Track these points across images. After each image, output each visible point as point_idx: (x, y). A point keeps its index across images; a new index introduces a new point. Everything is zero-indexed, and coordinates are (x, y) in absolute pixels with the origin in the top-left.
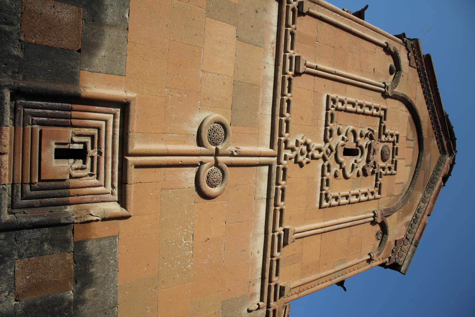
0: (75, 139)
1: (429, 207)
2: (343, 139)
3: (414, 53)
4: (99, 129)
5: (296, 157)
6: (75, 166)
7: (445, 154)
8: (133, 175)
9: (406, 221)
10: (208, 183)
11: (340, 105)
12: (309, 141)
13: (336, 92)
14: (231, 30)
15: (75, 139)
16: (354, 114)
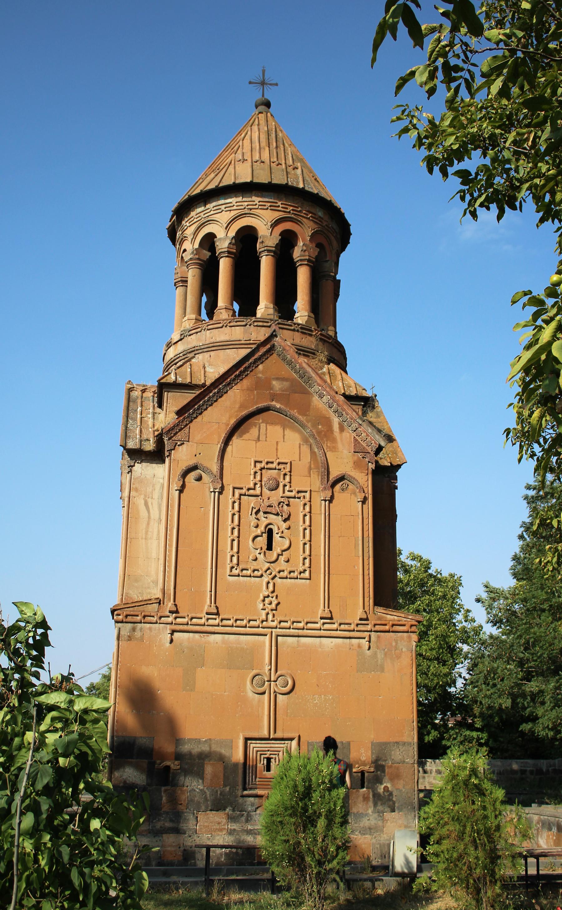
0: (262, 763)
1: (328, 389)
2: (260, 553)
3: (177, 433)
4: (257, 751)
5: (272, 610)
6: (274, 762)
7: (273, 346)
8: (279, 735)
9: (338, 430)
10: (285, 687)
11: (235, 559)
12: (262, 598)
13: (224, 564)
14: (200, 673)
15: (262, 763)
16: (240, 539)
